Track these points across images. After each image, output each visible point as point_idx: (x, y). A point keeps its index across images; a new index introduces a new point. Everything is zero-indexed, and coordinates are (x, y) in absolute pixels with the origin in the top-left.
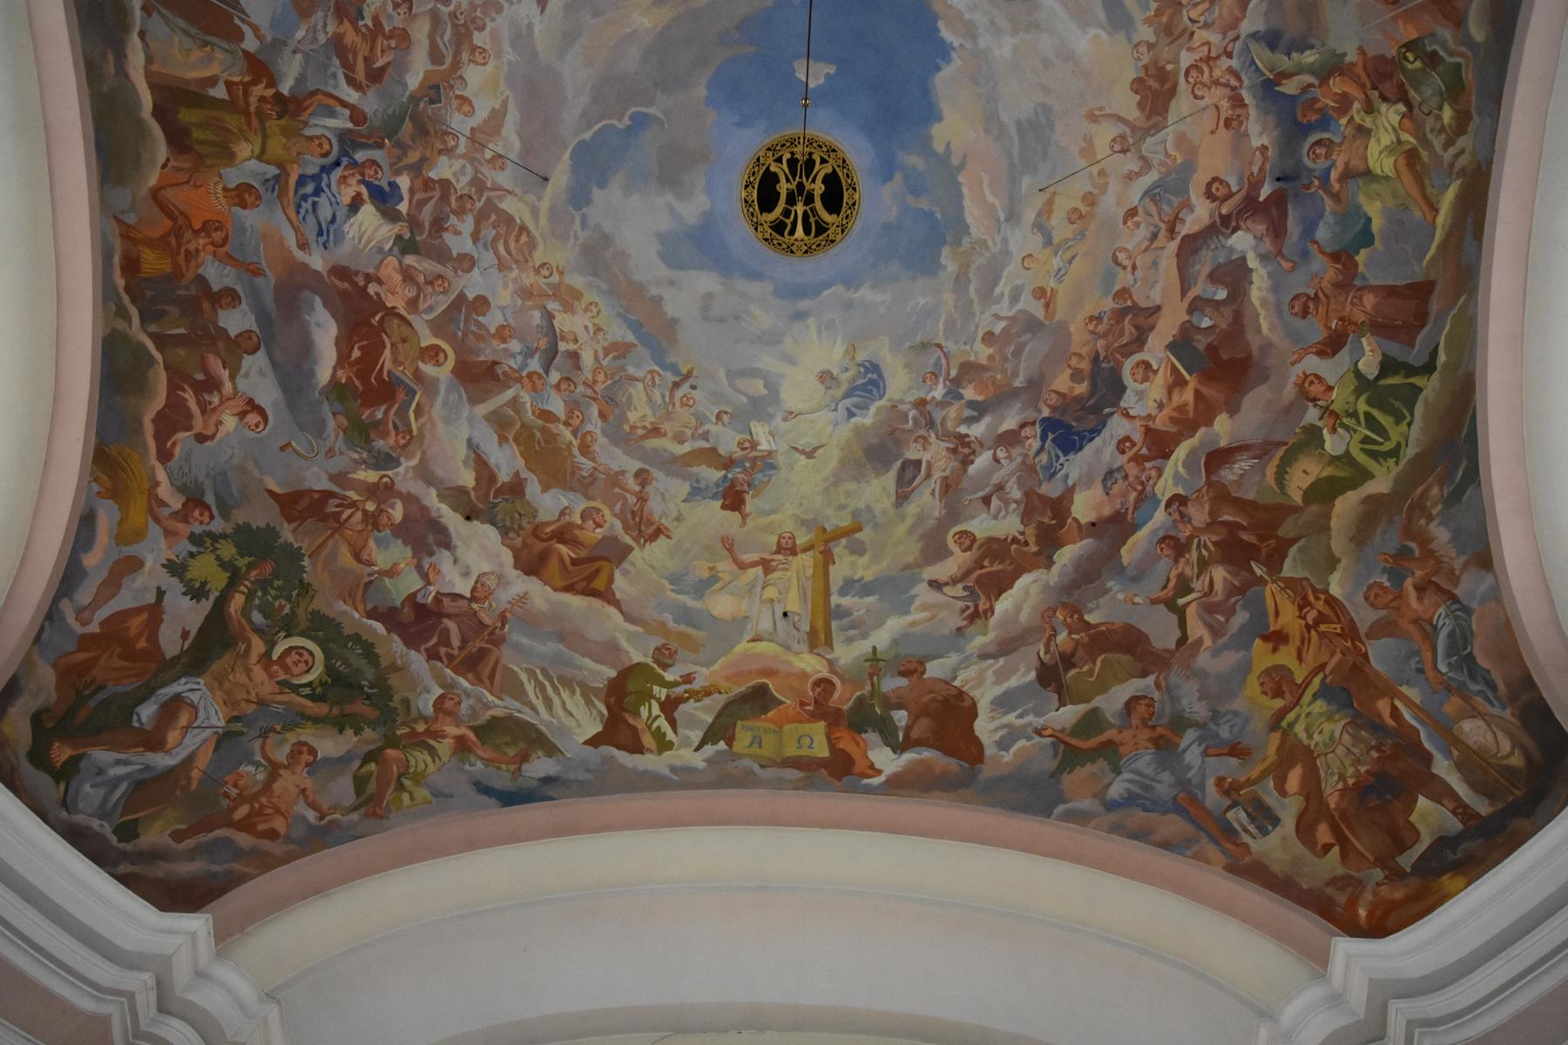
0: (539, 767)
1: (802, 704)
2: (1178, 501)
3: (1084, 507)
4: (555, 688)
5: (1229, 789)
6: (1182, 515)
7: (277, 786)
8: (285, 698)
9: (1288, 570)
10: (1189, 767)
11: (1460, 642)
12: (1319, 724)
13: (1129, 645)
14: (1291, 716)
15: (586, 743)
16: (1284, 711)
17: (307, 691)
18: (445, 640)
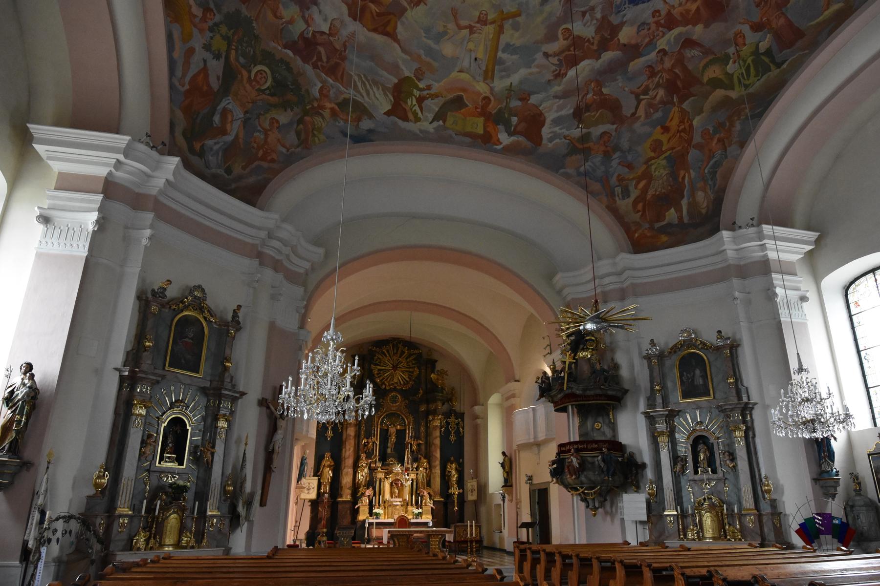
0: (366, 124)
1: (476, 108)
2: (663, 52)
3: (626, 35)
4: (370, 85)
5: (620, 179)
6: (662, 60)
7: (269, 140)
8: (261, 97)
9: (685, 106)
10: (612, 167)
11: (717, 165)
12: (660, 169)
13: (612, 107)
14: (653, 161)
15: (385, 114)
16: (654, 158)
17: (268, 92)
18: (320, 59)
